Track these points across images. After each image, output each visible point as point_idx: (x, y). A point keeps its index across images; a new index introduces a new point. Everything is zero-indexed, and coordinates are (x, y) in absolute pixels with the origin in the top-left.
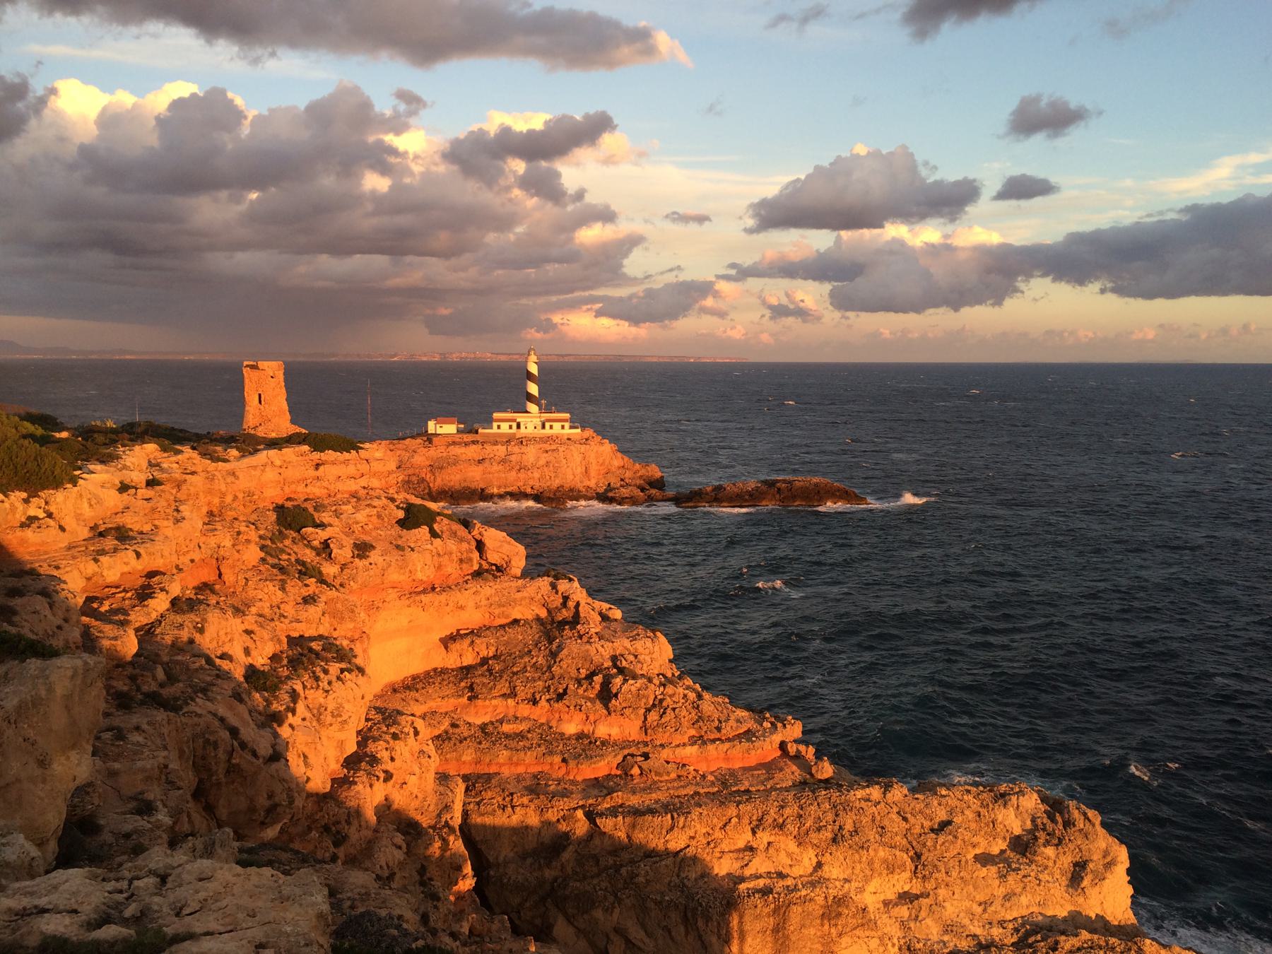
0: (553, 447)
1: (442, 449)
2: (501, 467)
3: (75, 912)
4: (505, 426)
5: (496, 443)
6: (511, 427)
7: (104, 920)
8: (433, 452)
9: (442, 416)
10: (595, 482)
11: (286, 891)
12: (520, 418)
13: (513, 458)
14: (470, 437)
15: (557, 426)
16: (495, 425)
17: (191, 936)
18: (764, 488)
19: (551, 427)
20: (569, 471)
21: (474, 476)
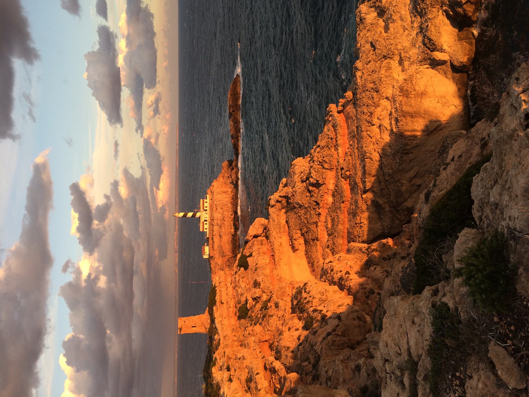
0: (215, 206)
1: (215, 252)
2: (223, 228)
3: (398, 394)
4: (206, 226)
5: (213, 230)
6: (206, 224)
7: (402, 383)
8: (217, 256)
9: (201, 252)
10: (229, 189)
11: (392, 313)
12: (202, 220)
13: (219, 223)
14: (210, 241)
15: (206, 205)
16: (205, 230)
17: (409, 350)
18: (232, 117)
19: (206, 207)
20: (225, 200)
21: (227, 239)
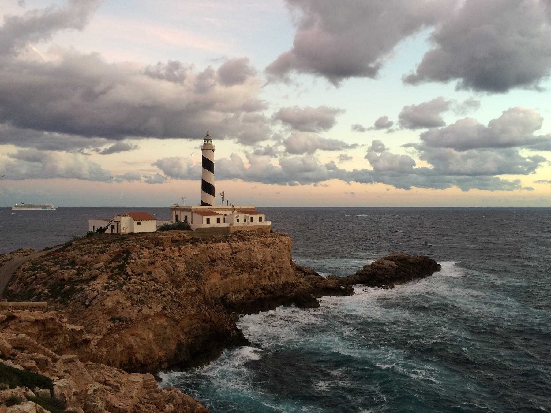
0: (270, 240)
4: (213, 219)
5: (216, 241)
6: (219, 221)
13: (241, 256)
15: (256, 217)
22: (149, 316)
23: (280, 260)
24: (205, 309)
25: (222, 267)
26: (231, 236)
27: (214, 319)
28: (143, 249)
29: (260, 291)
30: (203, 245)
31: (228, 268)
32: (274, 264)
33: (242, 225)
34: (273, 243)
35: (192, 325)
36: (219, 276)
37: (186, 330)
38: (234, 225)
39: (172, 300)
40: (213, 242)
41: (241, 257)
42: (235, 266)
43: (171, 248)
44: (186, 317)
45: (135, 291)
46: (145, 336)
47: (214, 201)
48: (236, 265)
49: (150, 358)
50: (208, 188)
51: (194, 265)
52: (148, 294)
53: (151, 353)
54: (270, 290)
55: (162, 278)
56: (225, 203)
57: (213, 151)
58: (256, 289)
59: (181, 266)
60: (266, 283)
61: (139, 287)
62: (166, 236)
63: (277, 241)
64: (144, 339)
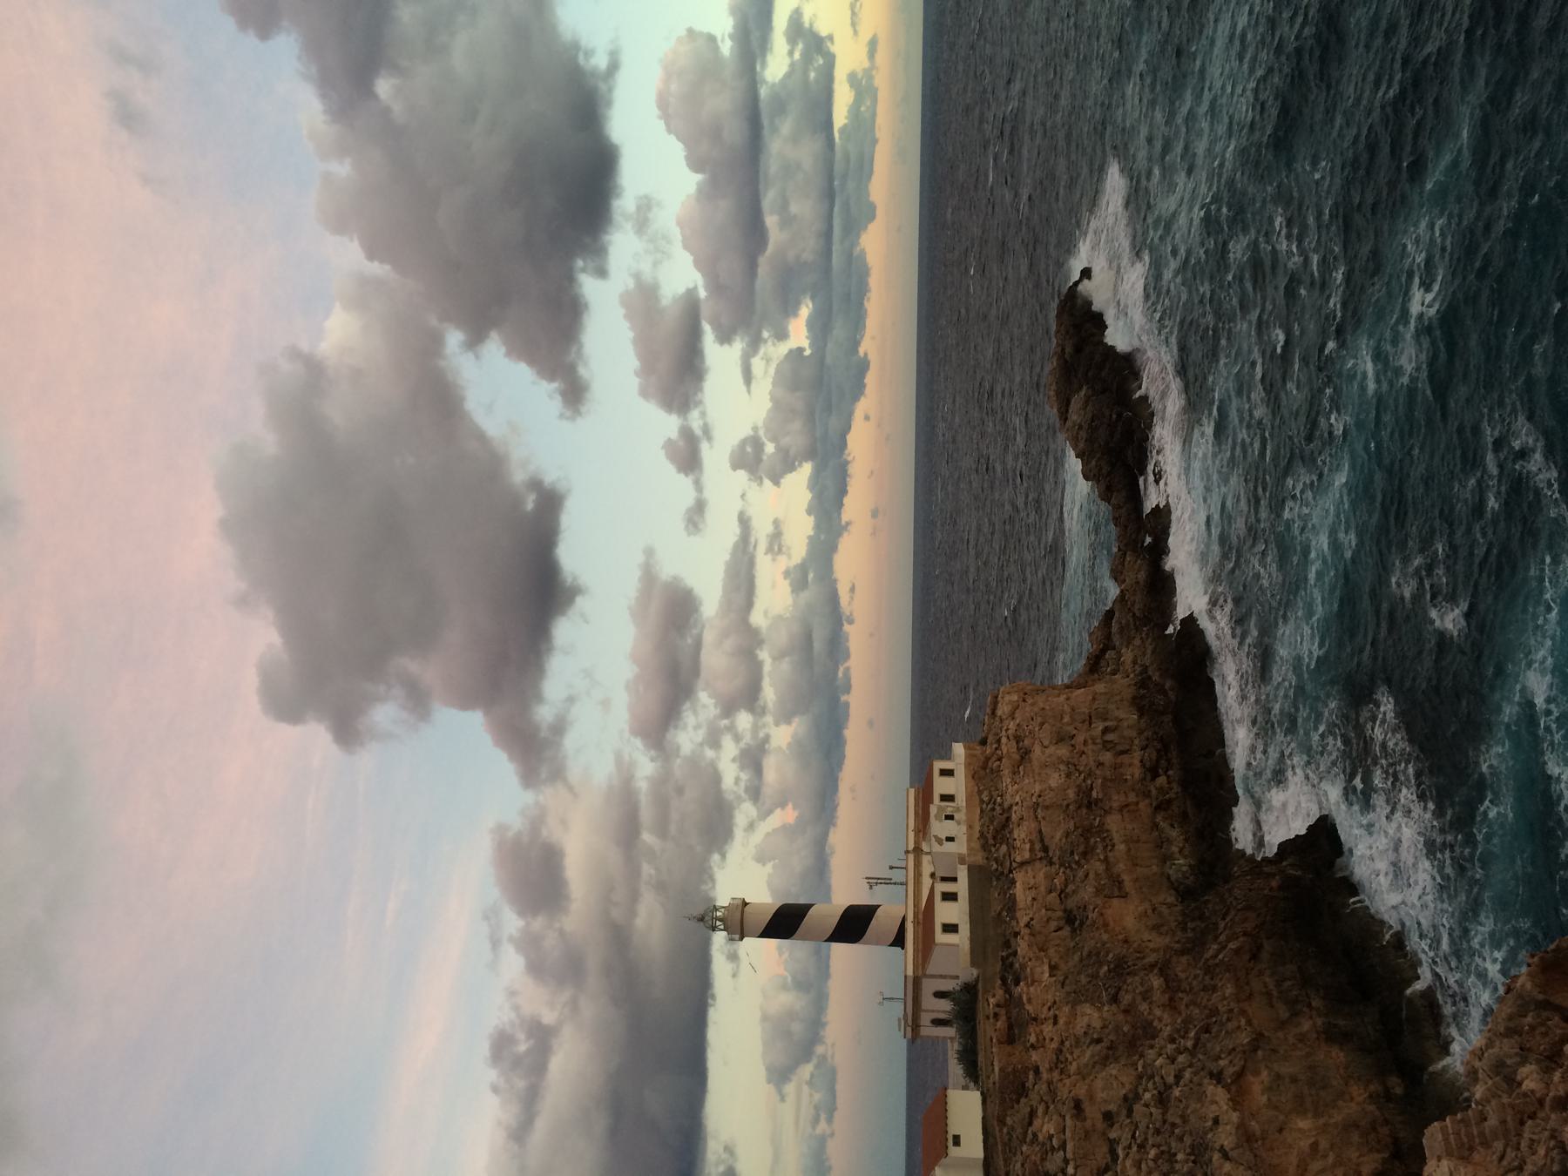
0: (1008, 747)
4: (946, 912)
5: (1011, 906)
6: (950, 897)
15: (942, 785)
22: (1241, 1126)
23: (1066, 720)
24: (1219, 951)
25: (1087, 893)
26: (996, 860)
27: (1249, 926)
28: (1035, 1135)
29: (1162, 780)
30: (1022, 947)
31: (1091, 876)
32: (1080, 738)
33: (964, 828)
34: (1018, 739)
35: (1269, 994)
36: (1115, 902)
37: (1284, 1013)
38: (964, 850)
39: (1192, 1052)
40: (1013, 918)
41: (1058, 835)
42: (1084, 854)
43: (1032, 1046)
44: (1243, 1012)
45: (1165, 1168)
46: (1305, 1144)
47: (893, 907)
48: (1082, 848)
49: (1374, 1129)
50: (853, 925)
51: (1084, 979)
52: (1174, 1125)
53: (1357, 1127)
54: (1158, 751)
55: (1124, 1079)
56: (898, 876)
57: (745, 904)
58: (1154, 792)
59: (1086, 1019)
60: (1137, 762)
61: (1153, 1153)
62: (995, 1060)
63: (1012, 726)
64: (1314, 1147)
